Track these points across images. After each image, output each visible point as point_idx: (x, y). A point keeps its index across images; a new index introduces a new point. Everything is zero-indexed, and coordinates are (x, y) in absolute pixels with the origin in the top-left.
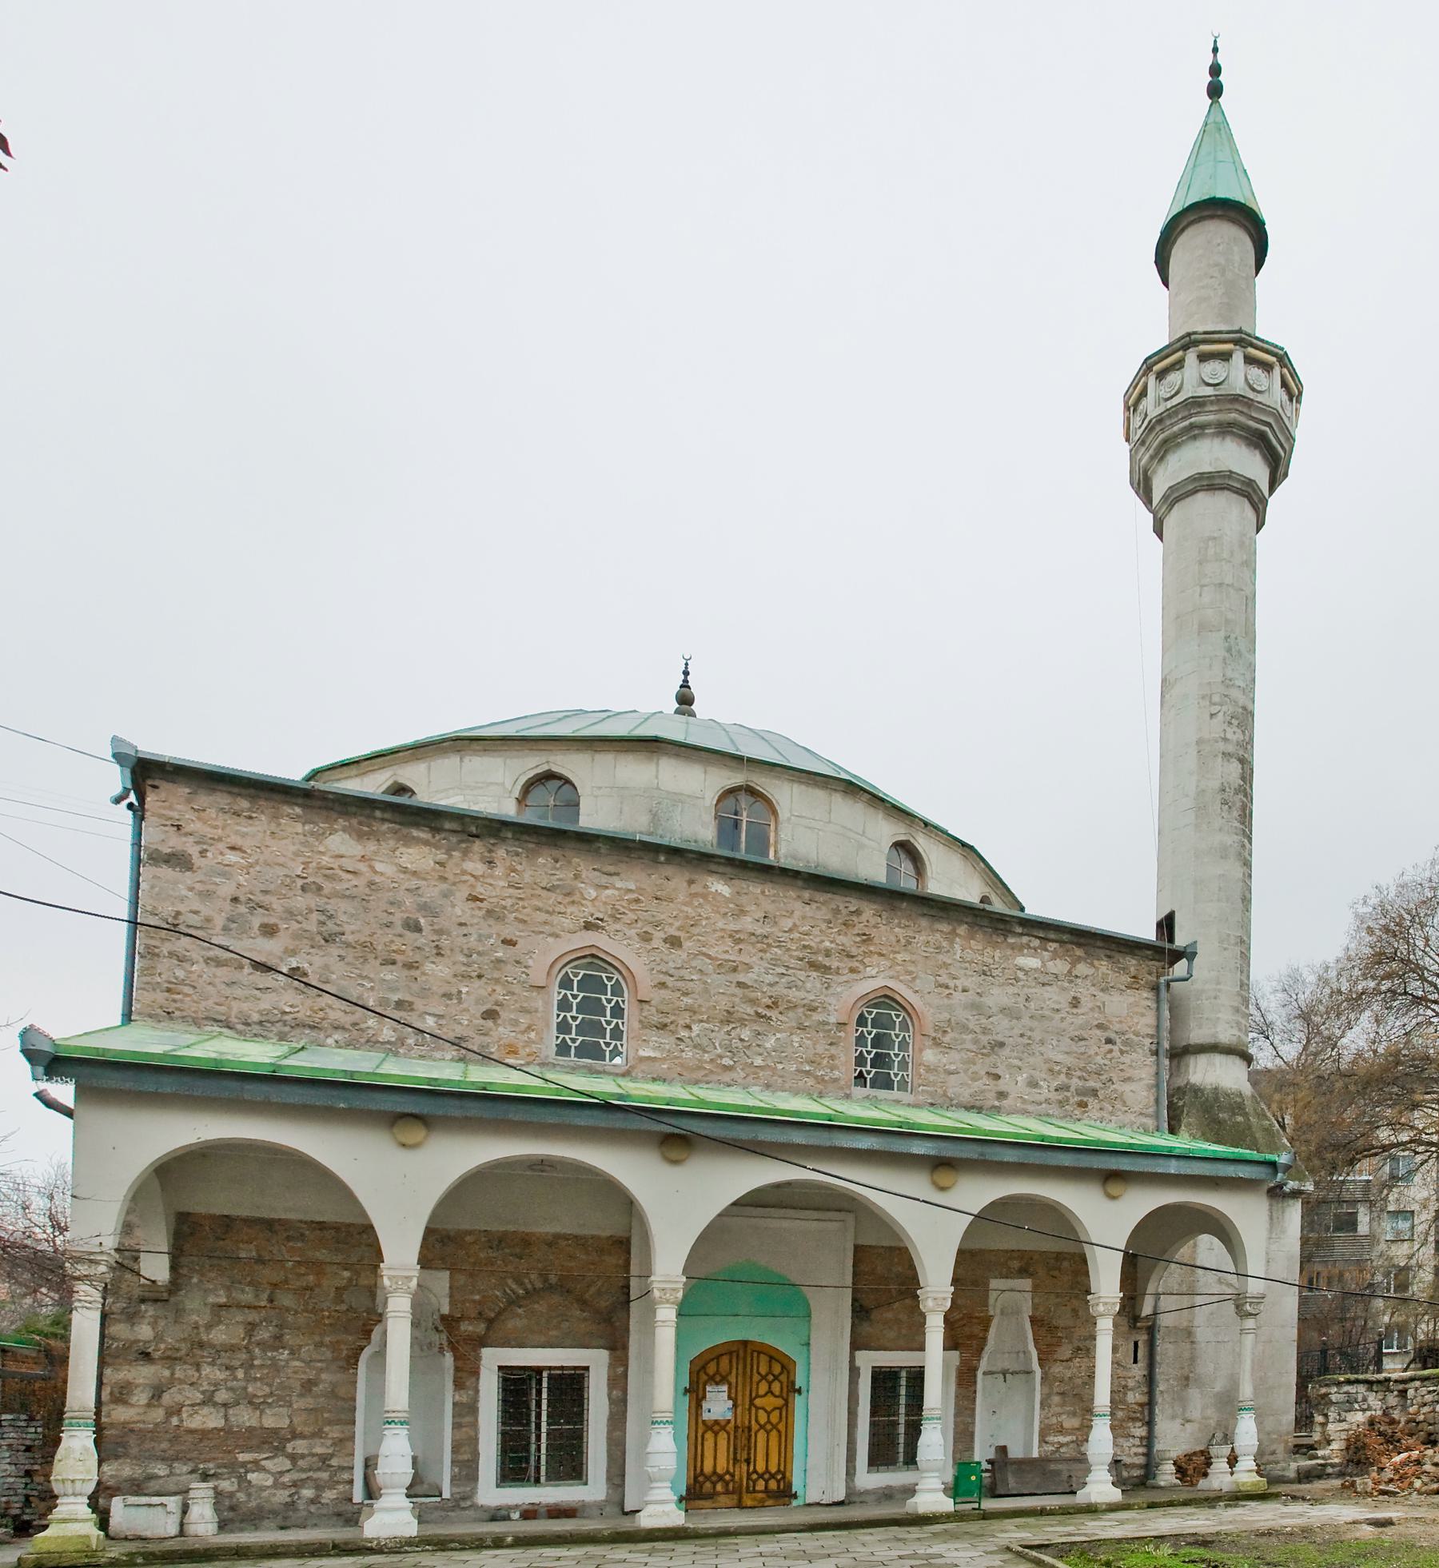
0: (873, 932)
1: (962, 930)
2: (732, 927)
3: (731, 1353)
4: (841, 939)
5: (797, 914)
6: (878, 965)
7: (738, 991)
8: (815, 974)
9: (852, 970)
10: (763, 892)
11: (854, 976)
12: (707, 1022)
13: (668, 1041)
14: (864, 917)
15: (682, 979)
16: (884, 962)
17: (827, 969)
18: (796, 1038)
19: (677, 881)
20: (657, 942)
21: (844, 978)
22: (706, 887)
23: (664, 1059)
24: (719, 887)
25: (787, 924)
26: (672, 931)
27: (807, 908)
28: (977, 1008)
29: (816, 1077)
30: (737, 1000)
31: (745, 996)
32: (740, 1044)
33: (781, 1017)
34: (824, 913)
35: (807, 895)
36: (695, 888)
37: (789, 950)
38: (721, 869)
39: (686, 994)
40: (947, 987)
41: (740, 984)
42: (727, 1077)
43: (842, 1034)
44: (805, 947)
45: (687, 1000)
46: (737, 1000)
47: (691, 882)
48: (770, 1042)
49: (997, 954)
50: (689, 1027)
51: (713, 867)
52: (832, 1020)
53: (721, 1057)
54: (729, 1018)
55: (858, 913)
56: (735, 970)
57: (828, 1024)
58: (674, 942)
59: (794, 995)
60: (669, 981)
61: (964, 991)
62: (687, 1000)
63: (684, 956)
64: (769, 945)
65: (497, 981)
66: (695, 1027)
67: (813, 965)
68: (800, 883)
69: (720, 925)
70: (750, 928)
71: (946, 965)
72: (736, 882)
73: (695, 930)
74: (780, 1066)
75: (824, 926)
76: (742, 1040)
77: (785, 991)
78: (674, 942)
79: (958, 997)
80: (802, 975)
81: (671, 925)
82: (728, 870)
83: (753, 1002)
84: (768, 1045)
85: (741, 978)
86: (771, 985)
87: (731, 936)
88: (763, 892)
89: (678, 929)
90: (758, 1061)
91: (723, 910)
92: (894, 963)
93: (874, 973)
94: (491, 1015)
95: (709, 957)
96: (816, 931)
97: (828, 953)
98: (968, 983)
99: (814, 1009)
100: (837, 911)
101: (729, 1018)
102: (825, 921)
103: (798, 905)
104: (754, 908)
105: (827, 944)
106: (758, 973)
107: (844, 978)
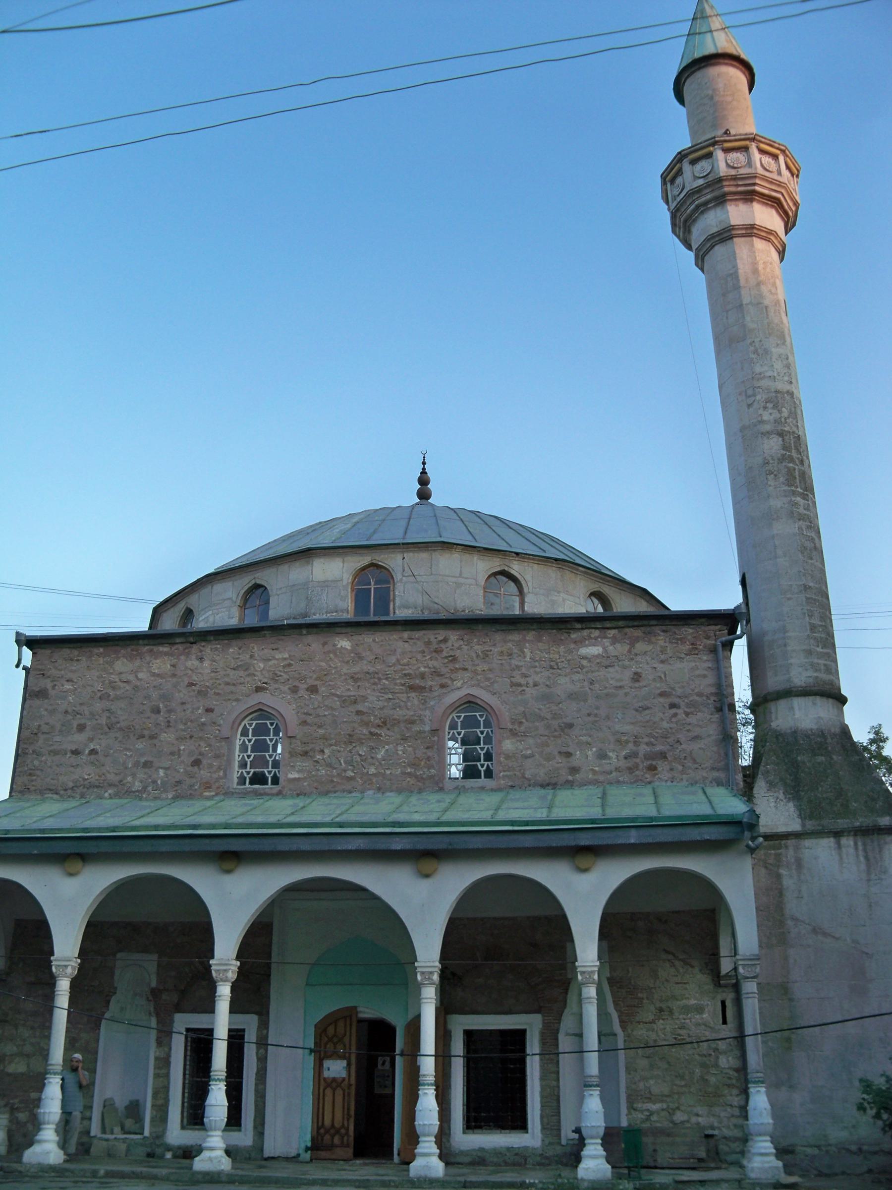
0: (458, 653)
1: (531, 635)
2: (356, 669)
3: (345, 1018)
4: (431, 664)
5: (399, 651)
6: (462, 678)
7: (356, 718)
8: (413, 694)
9: (443, 686)
10: (374, 641)
11: (444, 690)
12: (335, 745)
13: (307, 764)
14: (449, 644)
15: (318, 716)
16: (467, 675)
17: (421, 689)
18: (400, 748)
19: (314, 643)
20: (302, 693)
21: (436, 694)
22: (335, 645)
23: (305, 778)
24: (344, 643)
25: (393, 659)
26: (311, 682)
27: (406, 645)
28: (546, 698)
29: (416, 777)
30: (356, 725)
31: (362, 721)
32: (358, 759)
33: (388, 733)
34: (420, 645)
35: (406, 635)
36: (327, 648)
37: (394, 679)
38: (344, 630)
39: (320, 727)
40: (520, 685)
41: (358, 713)
42: (348, 787)
43: (436, 738)
44: (405, 675)
45: (321, 731)
46: (356, 725)
47: (324, 644)
48: (380, 754)
49: (562, 649)
50: (322, 751)
51: (338, 630)
52: (427, 728)
53: (345, 771)
54: (351, 739)
55: (445, 640)
56: (355, 702)
57: (424, 732)
58: (313, 690)
59: (399, 713)
60: (309, 719)
61: (536, 685)
62: (321, 731)
63: (320, 699)
64: (379, 679)
65: (201, 738)
66: (326, 751)
67: (412, 688)
68: (400, 628)
69: (345, 670)
70: (365, 668)
71: (518, 667)
72: (355, 638)
73: (328, 678)
74: (388, 772)
75: (419, 656)
76: (360, 755)
77: (391, 712)
78: (313, 690)
79: (530, 692)
80: (403, 697)
81: (311, 677)
82: (349, 630)
83: (367, 724)
84: (379, 756)
85: (360, 707)
86: (381, 709)
87: (352, 677)
88: (374, 641)
89: (316, 679)
90: (372, 770)
91: (346, 659)
92: (475, 672)
93: (459, 685)
94: (197, 763)
95: (338, 696)
96: (413, 661)
97: (422, 676)
98: (537, 678)
99: (412, 722)
100: (428, 643)
101: (351, 739)
102: (420, 652)
103: (400, 643)
104: (368, 653)
105: (422, 669)
106: (373, 700)
107: (436, 694)
